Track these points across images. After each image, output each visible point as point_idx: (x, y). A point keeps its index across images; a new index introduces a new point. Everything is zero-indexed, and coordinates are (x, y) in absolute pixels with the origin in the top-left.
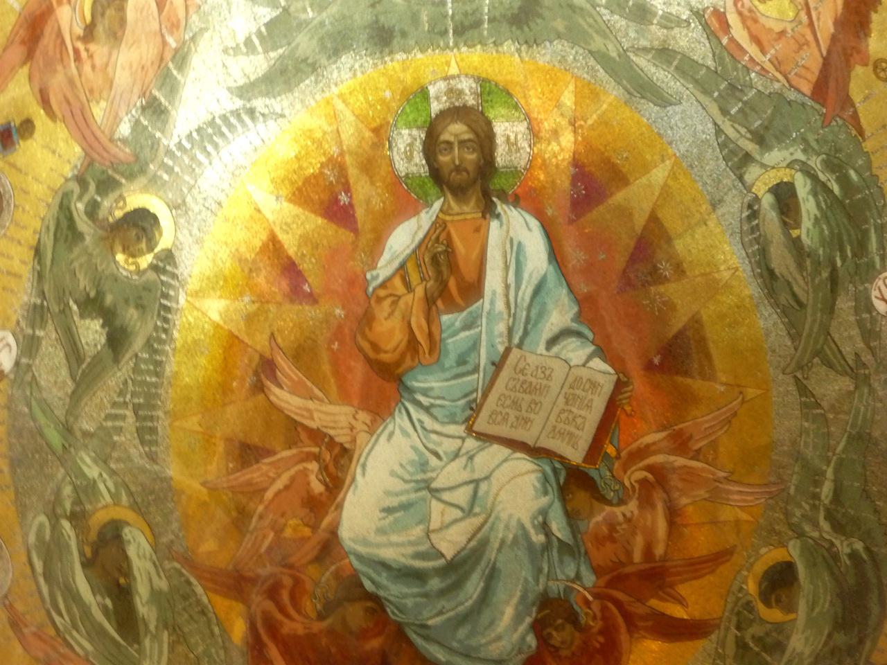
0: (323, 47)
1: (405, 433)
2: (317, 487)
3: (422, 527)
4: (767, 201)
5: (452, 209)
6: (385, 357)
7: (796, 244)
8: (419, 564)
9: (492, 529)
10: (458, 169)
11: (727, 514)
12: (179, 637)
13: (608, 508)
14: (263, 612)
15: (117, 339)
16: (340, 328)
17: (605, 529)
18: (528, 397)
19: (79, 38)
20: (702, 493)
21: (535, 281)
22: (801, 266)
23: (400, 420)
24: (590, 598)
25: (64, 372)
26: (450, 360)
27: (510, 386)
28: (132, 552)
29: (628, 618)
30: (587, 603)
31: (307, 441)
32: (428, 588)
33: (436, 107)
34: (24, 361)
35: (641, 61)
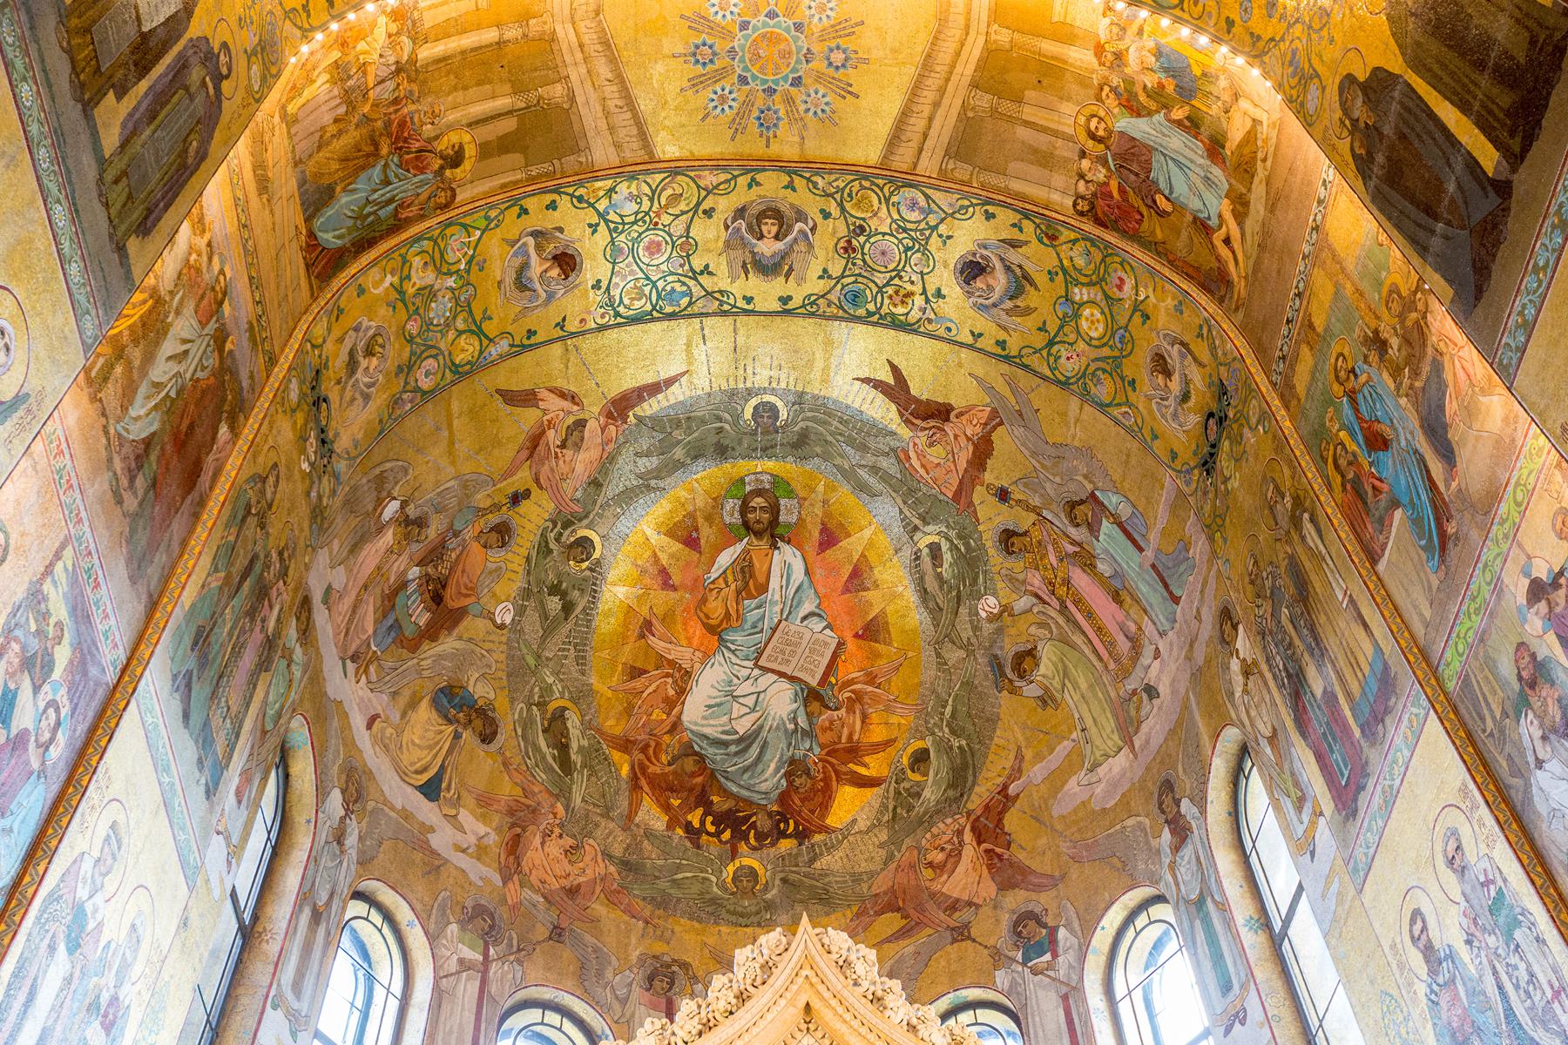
0: (688, 454)
1: (720, 664)
2: (671, 692)
4: (926, 551)
6: (711, 622)
7: (939, 576)
10: (758, 522)
12: (593, 773)
15: (568, 608)
17: (827, 724)
21: (796, 585)
22: (941, 588)
23: (719, 658)
25: (538, 624)
26: (748, 625)
28: (569, 724)
30: (815, 763)
33: (748, 488)
35: (861, 472)
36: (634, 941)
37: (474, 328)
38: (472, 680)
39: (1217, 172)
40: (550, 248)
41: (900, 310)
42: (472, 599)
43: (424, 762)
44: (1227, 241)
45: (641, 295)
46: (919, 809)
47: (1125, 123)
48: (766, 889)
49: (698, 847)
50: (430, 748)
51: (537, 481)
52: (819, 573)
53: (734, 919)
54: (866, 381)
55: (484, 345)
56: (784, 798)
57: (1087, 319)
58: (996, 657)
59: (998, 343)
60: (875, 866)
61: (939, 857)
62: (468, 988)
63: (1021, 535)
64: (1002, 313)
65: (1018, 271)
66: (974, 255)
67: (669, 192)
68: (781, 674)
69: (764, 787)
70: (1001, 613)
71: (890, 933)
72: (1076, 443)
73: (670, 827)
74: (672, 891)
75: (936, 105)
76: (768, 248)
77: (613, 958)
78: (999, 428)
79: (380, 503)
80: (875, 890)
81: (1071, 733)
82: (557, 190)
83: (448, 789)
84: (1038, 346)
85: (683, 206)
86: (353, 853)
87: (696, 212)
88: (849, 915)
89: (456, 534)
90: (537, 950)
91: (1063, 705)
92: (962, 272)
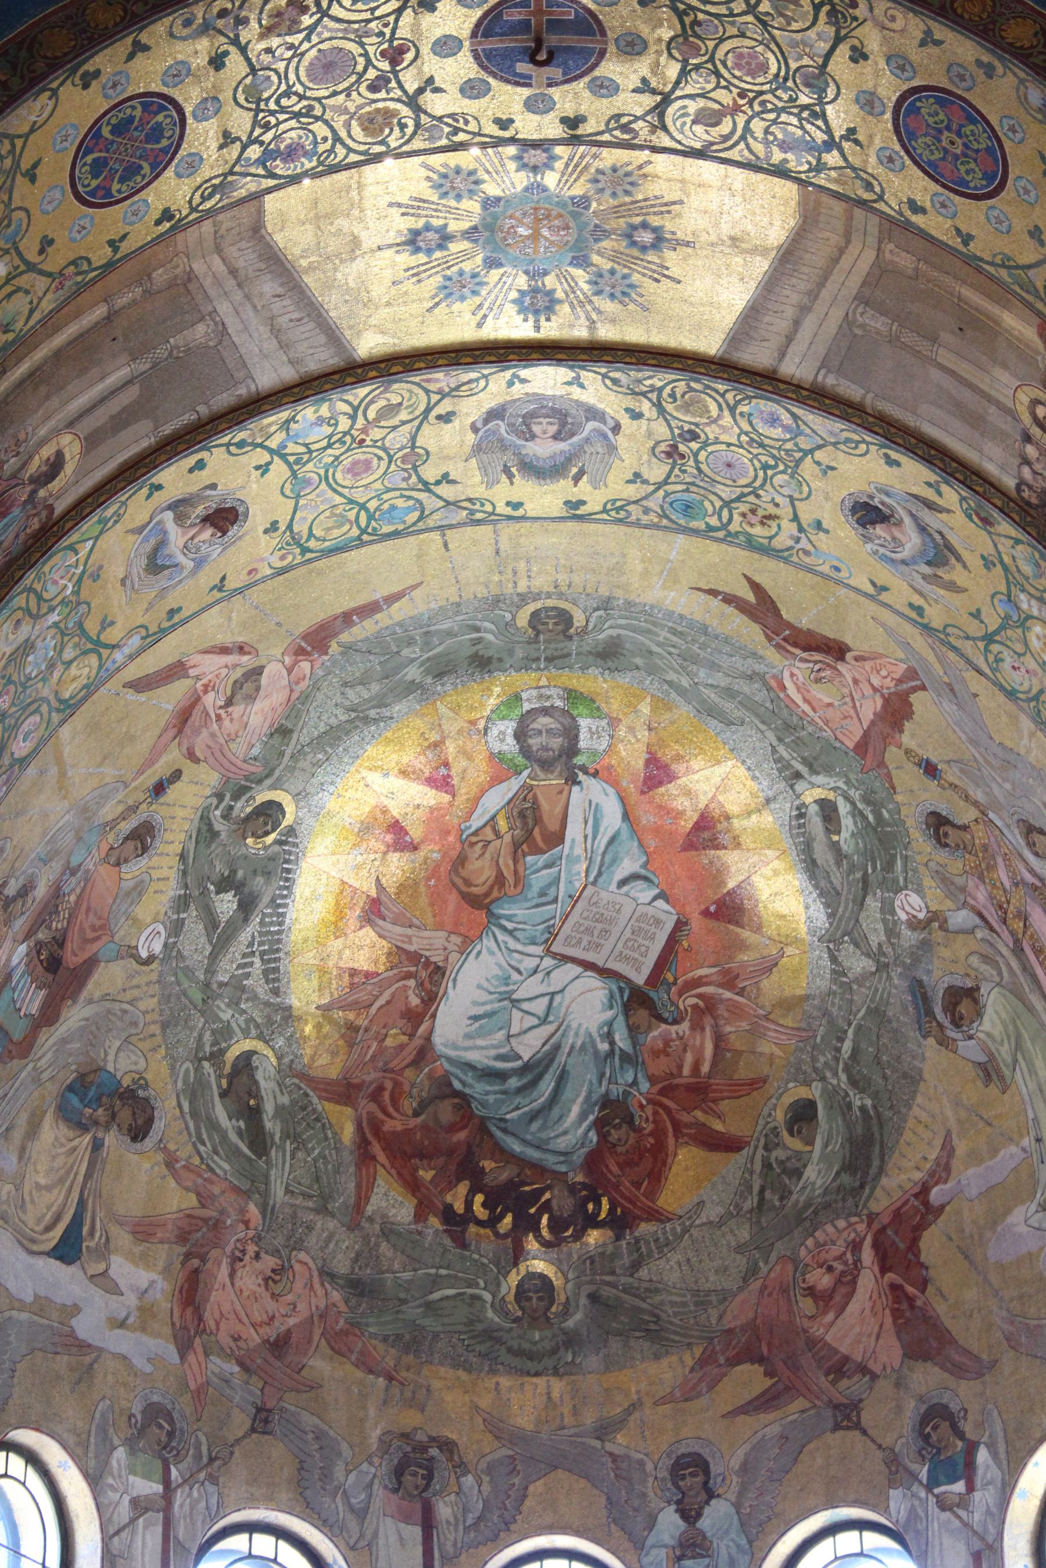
0: (427, 672)
1: (492, 953)
2: (415, 1001)
3: (503, 1032)
4: (814, 809)
5: (536, 775)
6: (475, 890)
7: (835, 847)
8: (500, 1065)
9: (563, 1035)
10: (545, 749)
11: (765, 1047)
12: (300, 1143)
13: (664, 1026)
14: (368, 1113)
15: (246, 906)
16: (438, 865)
17: (660, 1044)
18: (599, 926)
19: (221, 707)
20: (744, 1025)
21: (610, 834)
22: (839, 864)
23: (488, 942)
24: (644, 1102)
25: (203, 939)
27: (585, 914)
28: (259, 1076)
29: (677, 1125)
30: (642, 1107)
31: (406, 963)
32: (507, 1086)
33: (527, 707)
34: (171, 940)
36: (372, 1412)
37: (89, 646)
38: (112, 1053)
40: (200, 510)
41: (758, 531)
42: (105, 938)
43: (54, 1209)
45: (342, 520)
46: (798, 1197)
48: (566, 1313)
49: (463, 1245)
50: (61, 1181)
52: (647, 818)
53: (516, 1362)
54: (713, 593)
55: (104, 657)
56: (593, 1161)
57: (1038, 638)
58: (920, 983)
59: (911, 605)
60: (731, 1283)
61: (823, 1281)
63: (959, 828)
64: (919, 579)
65: (938, 537)
66: (872, 497)
67: (382, 403)
68: (588, 966)
69: (562, 1143)
70: (929, 922)
71: (748, 1397)
72: (1032, 759)
73: (420, 1216)
74: (427, 1322)
75: (804, 310)
76: (543, 449)
77: (344, 1446)
78: (920, 694)
80: (727, 1323)
81: (1021, 1136)
83: (92, 1233)
84: (972, 634)
85: (404, 416)
87: (426, 418)
88: (689, 1362)
89: (73, 873)
90: (237, 1454)
91: (1013, 1088)
92: (854, 510)
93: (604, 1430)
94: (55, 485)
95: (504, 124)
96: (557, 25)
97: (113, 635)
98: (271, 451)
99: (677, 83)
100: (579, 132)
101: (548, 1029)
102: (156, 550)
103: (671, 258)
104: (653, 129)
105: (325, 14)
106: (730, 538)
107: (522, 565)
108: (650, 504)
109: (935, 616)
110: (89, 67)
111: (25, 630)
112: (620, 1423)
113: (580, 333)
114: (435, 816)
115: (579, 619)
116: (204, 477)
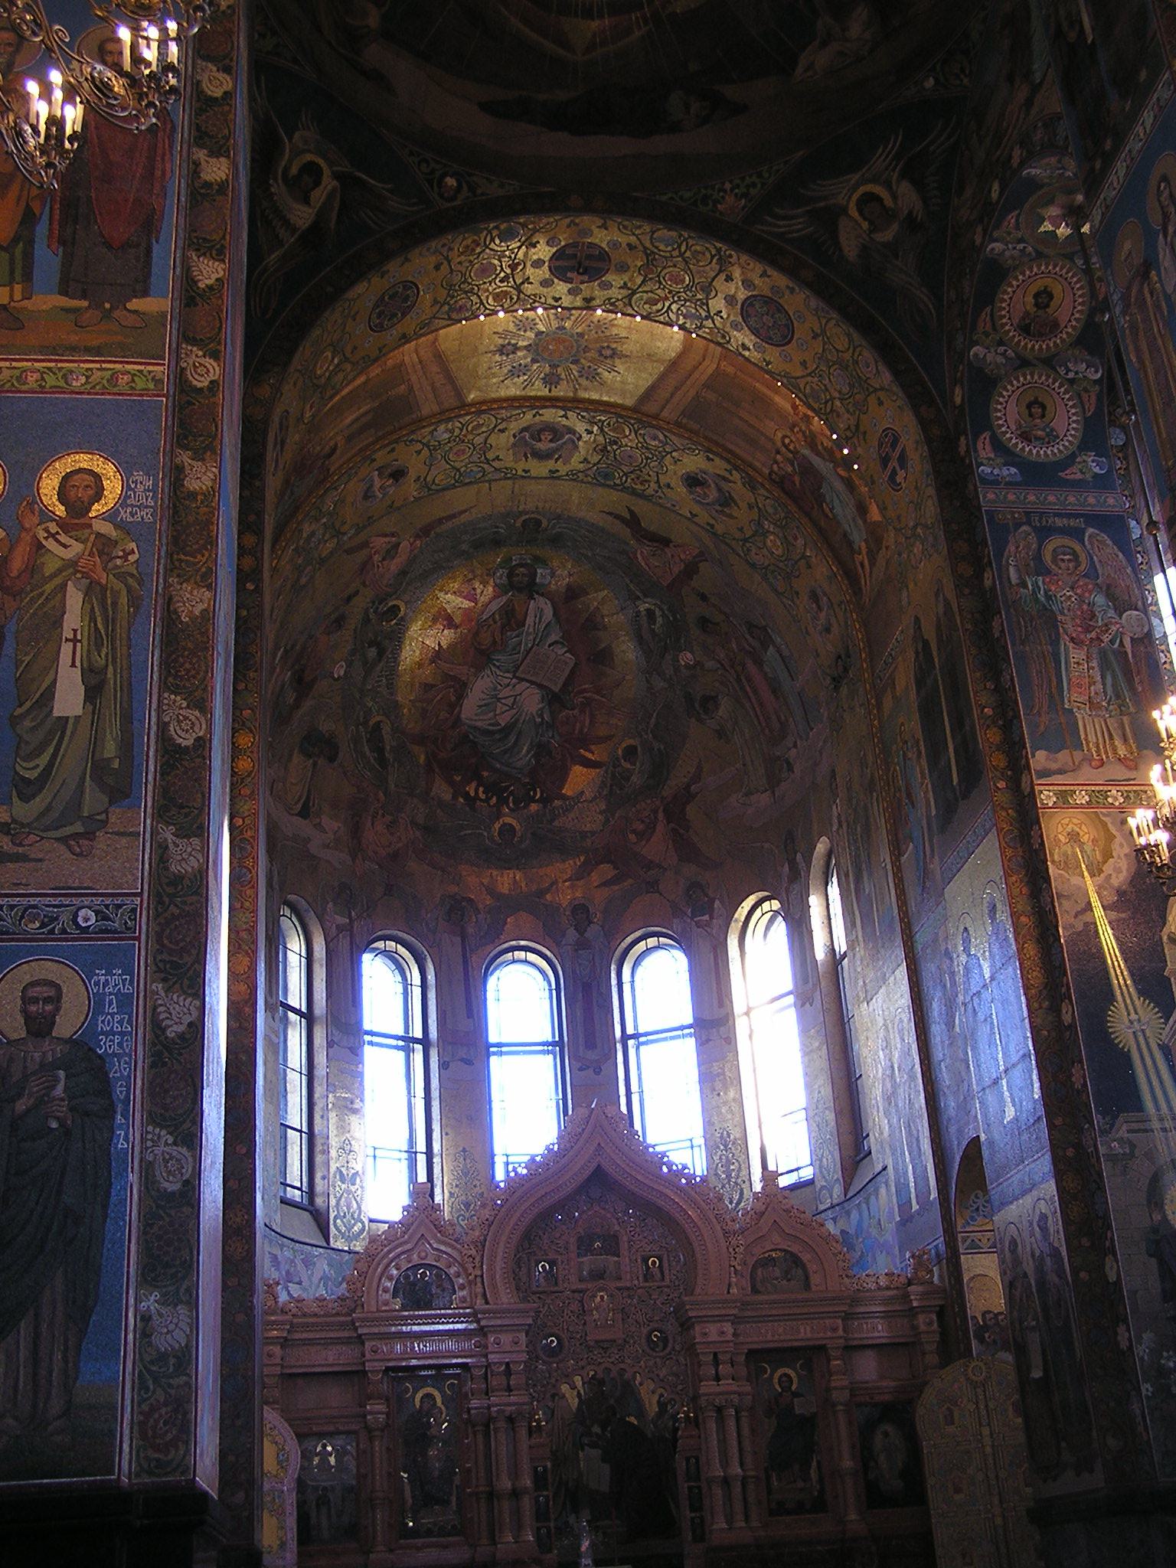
2: (453, 699)
8: (491, 728)
15: (381, 653)
33: (514, 563)
39: (860, 522)
41: (639, 487)
44: (862, 565)
47: (806, 452)
51: (364, 584)
59: (708, 524)
62: (344, 944)
69: (519, 764)
70: (694, 666)
73: (455, 797)
75: (677, 389)
79: (274, 658)
82: (396, 441)
85: (484, 429)
86: (277, 887)
93: (541, 893)
94: (334, 457)
95: (557, 300)
96: (590, 257)
97: (346, 527)
98: (424, 444)
99: (640, 286)
100: (591, 304)
101: (515, 711)
102: (368, 489)
103: (617, 361)
104: (625, 305)
105: (487, 247)
106: (624, 489)
107: (522, 498)
108: (589, 472)
109: (720, 529)
110: (385, 269)
111: (313, 526)
112: (548, 890)
113: (572, 394)
114: (467, 612)
115: (545, 523)
116: (394, 455)
